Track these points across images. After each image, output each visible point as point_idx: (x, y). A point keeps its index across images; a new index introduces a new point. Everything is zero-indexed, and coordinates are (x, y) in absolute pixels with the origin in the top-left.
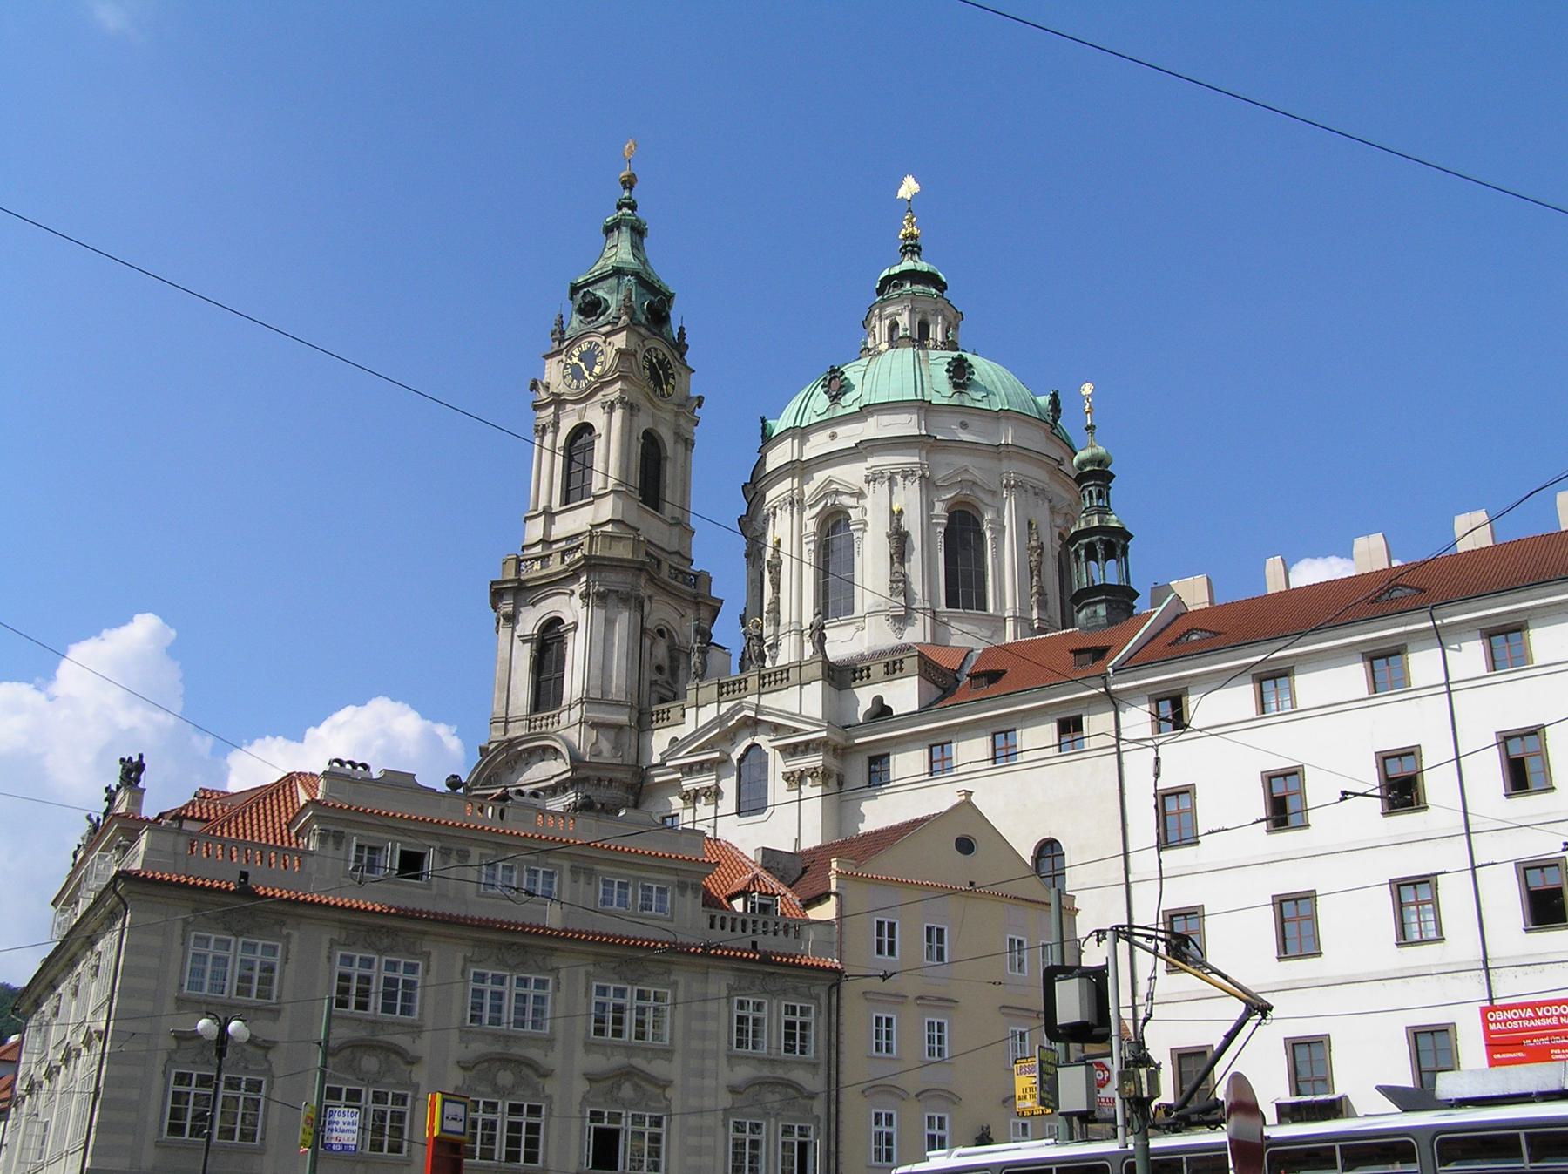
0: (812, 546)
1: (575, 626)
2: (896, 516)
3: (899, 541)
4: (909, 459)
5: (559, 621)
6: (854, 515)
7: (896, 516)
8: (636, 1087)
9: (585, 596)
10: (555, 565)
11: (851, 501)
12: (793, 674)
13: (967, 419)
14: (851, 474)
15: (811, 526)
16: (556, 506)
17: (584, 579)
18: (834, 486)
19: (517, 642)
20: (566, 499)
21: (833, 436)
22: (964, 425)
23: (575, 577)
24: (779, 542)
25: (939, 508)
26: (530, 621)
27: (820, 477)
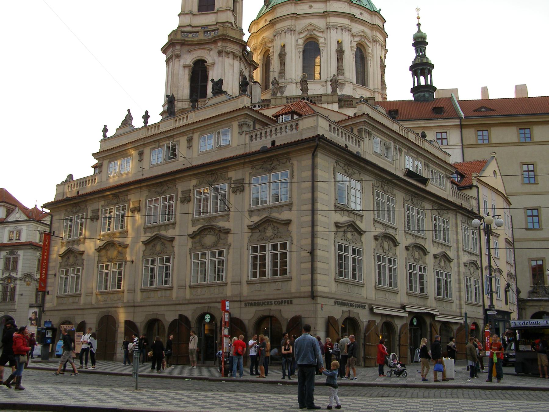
0: (301, 50)
1: (214, 64)
2: (339, 44)
3: (340, 53)
4: (345, 21)
5: (206, 62)
6: (321, 40)
7: (339, 44)
8: (445, 261)
9: (220, 53)
10: (201, 37)
11: (319, 34)
12: (324, 99)
13: (363, 12)
14: (320, 23)
15: (301, 42)
16: (195, 10)
17: (219, 44)
18: (311, 27)
19: (181, 68)
20: (199, 11)
21: (311, 7)
22: (361, 14)
23: (214, 41)
24: (284, 45)
25: (354, 44)
26: (189, 59)
27: (307, 21)
